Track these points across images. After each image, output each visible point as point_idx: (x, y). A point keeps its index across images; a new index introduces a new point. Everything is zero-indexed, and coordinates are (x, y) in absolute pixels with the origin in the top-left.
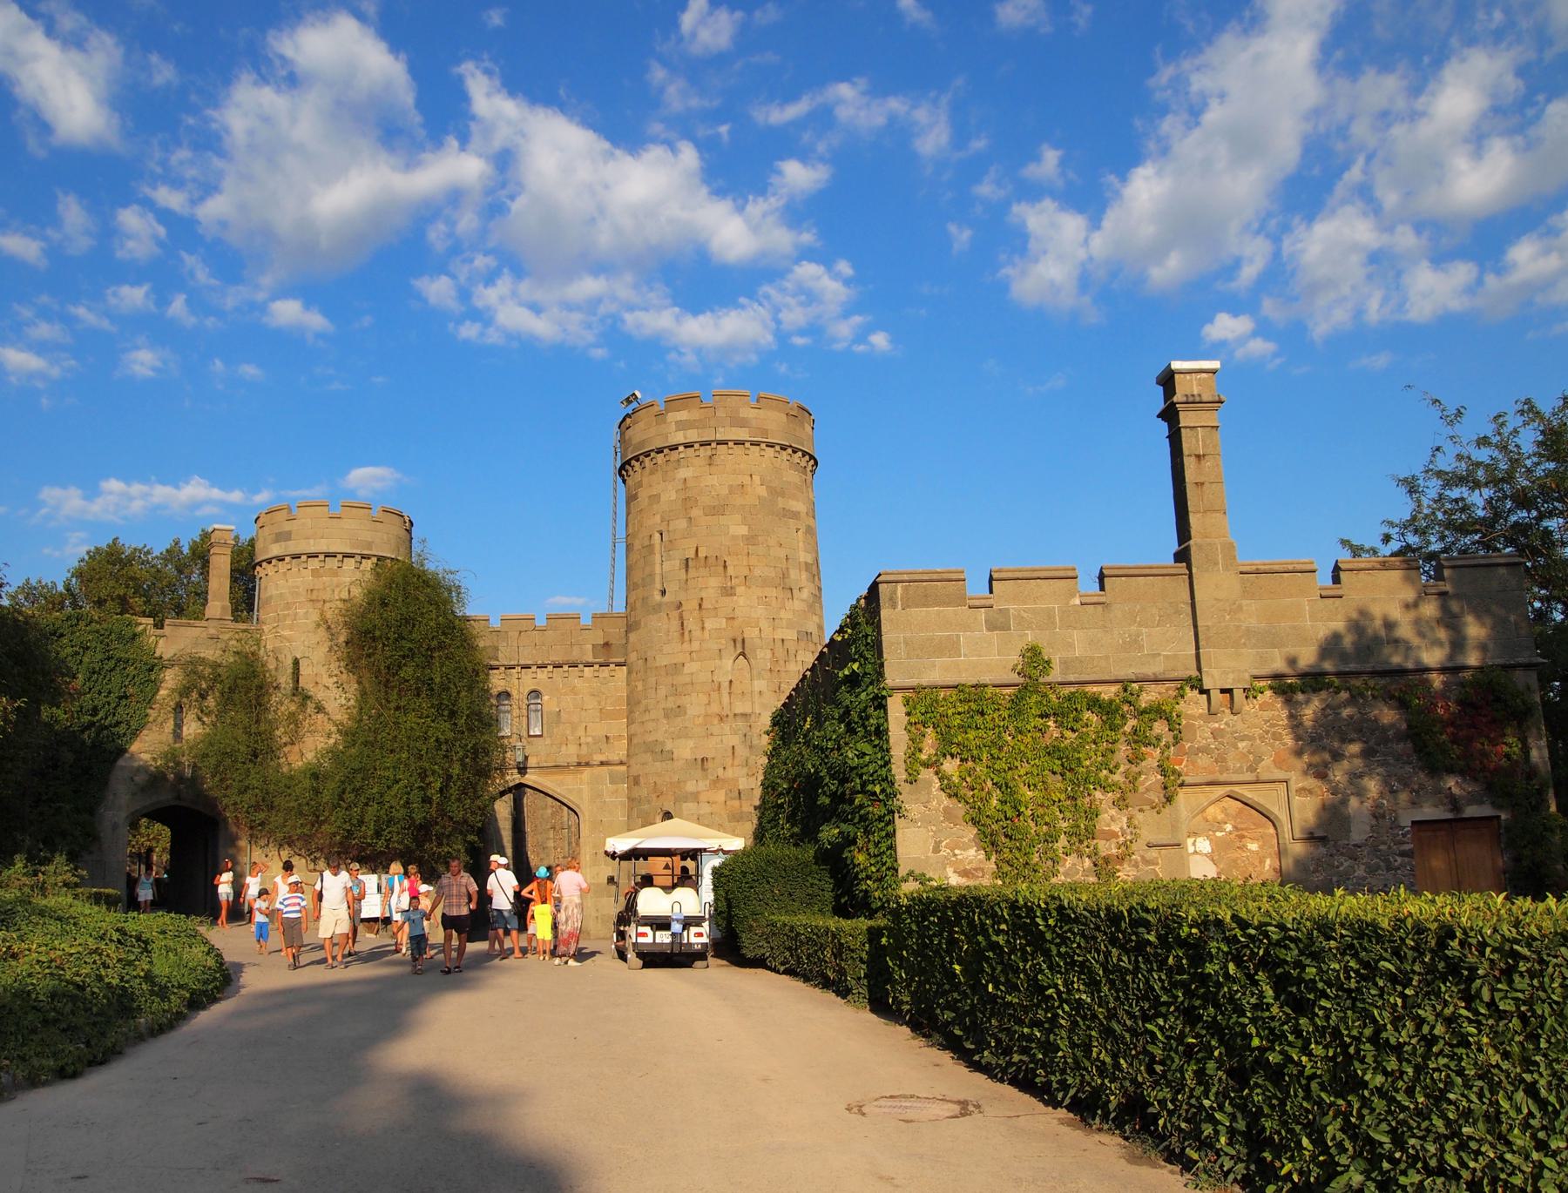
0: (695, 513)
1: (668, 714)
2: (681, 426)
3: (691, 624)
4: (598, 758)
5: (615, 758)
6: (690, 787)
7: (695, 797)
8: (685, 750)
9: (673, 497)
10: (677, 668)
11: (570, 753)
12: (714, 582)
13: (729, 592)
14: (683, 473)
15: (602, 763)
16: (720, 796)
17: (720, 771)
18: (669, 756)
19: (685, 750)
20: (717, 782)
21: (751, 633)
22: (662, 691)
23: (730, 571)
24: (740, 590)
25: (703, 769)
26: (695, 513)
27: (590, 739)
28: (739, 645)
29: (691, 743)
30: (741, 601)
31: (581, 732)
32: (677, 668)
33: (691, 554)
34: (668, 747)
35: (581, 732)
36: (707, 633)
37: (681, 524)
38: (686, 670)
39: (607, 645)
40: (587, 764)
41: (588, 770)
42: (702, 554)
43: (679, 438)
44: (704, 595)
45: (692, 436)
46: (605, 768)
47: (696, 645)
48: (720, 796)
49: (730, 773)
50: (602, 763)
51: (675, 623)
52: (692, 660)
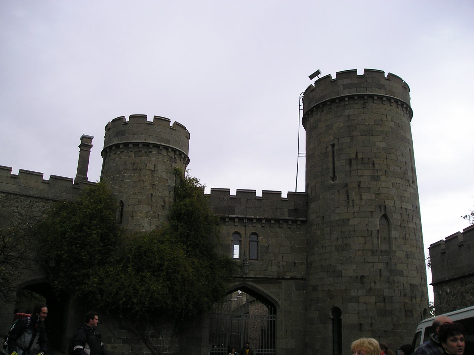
0: (355, 133)
2: (346, 87)
3: (354, 196)
4: (289, 275)
5: (299, 276)
6: (353, 293)
7: (357, 300)
8: (349, 271)
9: (342, 125)
10: (345, 222)
11: (273, 272)
12: (367, 172)
13: (376, 178)
14: (347, 112)
15: (292, 278)
16: (373, 299)
17: (372, 285)
19: (349, 271)
20: (370, 291)
21: (389, 203)
23: (377, 167)
24: (383, 178)
25: (362, 283)
26: (355, 133)
27: (285, 263)
28: (383, 209)
32: (345, 222)
33: (353, 156)
34: (339, 267)
36: (363, 202)
37: (348, 140)
38: (351, 223)
39: (296, 210)
40: (284, 279)
41: (284, 282)
42: (360, 156)
43: (346, 93)
44: (361, 179)
45: (354, 92)
47: (356, 209)
48: (373, 299)
49: (378, 286)
52: (354, 217)
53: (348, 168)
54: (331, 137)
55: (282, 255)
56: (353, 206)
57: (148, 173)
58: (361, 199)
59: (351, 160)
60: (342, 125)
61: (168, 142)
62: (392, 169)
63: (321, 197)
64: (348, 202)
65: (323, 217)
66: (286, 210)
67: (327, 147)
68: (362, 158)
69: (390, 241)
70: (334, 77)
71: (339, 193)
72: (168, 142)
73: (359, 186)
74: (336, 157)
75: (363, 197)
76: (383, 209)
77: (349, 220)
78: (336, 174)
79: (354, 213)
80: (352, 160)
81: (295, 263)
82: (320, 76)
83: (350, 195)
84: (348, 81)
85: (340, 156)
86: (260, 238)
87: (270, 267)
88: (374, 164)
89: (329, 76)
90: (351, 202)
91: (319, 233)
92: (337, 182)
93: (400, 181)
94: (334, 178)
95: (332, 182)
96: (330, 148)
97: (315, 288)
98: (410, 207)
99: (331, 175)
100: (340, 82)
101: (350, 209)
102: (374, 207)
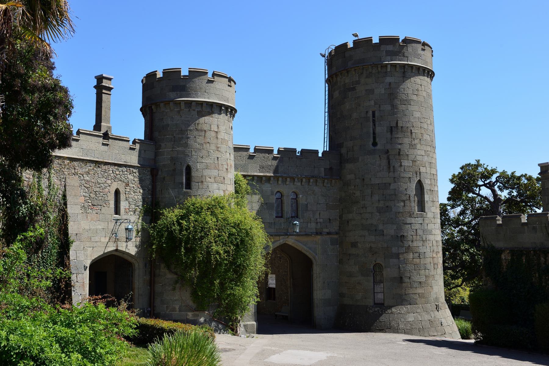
1: (379, 211)
4: (326, 230)
10: (387, 186)
14: (388, 79)
15: (328, 233)
17: (410, 243)
18: (382, 233)
19: (390, 231)
21: (423, 170)
22: (376, 198)
23: (414, 134)
24: (418, 146)
27: (321, 220)
28: (418, 175)
29: (395, 227)
30: (419, 152)
31: (317, 216)
32: (387, 186)
34: (381, 227)
35: (317, 216)
37: (388, 107)
38: (392, 187)
39: (331, 169)
46: (328, 236)
50: (328, 233)
51: (384, 162)
52: (395, 182)
53: (389, 135)
54: (372, 103)
55: (319, 212)
56: (394, 172)
57: (213, 134)
58: (401, 166)
59: (391, 127)
60: (383, 91)
61: (227, 100)
62: (424, 138)
63: (360, 159)
64: (389, 168)
65: (364, 179)
66: (323, 169)
67: (367, 112)
68: (402, 127)
69: (422, 203)
70: (376, 40)
71: (380, 159)
72: (227, 100)
73: (399, 152)
74: (377, 123)
75: (403, 164)
76: (418, 175)
77: (390, 184)
78: (377, 140)
79: (395, 178)
80: (393, 128)
81: (330, 219)
82: (360, 38)
83: (391, 161)
84: (390, 48)
85: (382, 122)
86: (301, 196)
87: (309, 225)
88: (411, 133)
89: (369, 40)
90: (392, 167)
91: (358, 193)
92: (379, 147)
93: (429, 148)
94: (375, 144)
95: (373, 148)
96: (370, 113)
97: (354, 245)
98: (433, 172)
99: (372, 140)
100: (383, 47)
101: (391, 174)
102: (411, 173)
